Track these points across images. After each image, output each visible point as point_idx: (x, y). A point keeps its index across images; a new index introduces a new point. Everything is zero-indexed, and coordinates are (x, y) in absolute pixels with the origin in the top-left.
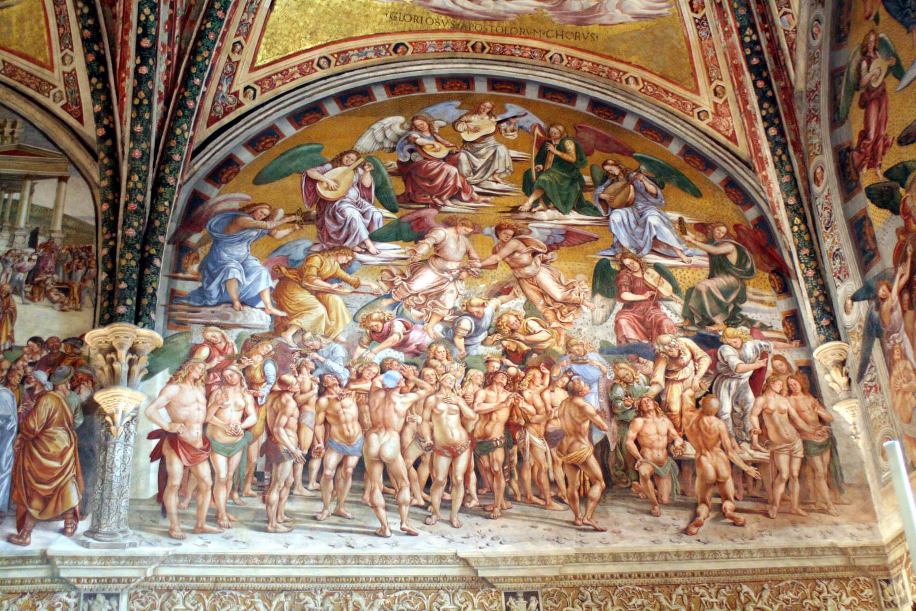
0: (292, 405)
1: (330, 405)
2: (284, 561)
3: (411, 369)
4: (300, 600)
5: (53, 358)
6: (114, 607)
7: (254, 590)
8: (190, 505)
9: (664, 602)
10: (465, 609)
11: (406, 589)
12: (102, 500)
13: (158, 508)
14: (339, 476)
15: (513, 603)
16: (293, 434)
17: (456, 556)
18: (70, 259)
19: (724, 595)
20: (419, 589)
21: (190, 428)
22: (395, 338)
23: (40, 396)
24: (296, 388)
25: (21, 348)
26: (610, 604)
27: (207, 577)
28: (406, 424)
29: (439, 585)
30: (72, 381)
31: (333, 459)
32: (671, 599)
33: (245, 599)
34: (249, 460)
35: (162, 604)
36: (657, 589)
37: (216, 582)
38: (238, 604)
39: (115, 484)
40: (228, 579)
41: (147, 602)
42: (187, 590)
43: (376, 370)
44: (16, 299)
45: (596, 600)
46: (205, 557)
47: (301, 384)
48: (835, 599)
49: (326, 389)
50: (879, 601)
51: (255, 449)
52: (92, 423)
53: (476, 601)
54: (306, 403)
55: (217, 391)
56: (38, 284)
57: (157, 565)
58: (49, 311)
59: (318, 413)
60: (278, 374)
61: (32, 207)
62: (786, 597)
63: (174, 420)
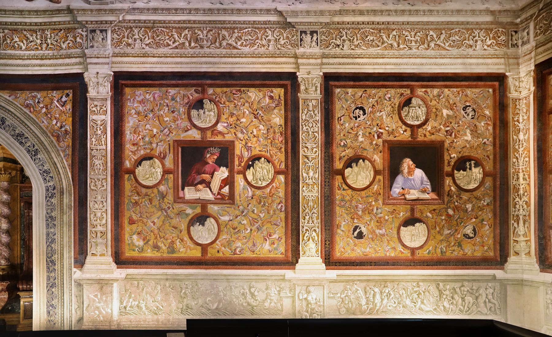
2: (188, 12)
4: (195, 33)
6: (105, 36)
7: (173, 28)
9: (385, 39)
10: (279, 39)
11: (249, 28)
15: (304, 37)
17: (276, 9)
19: (419, 36)
20: (255, 28)
26: (355, 39)
27: (150, 21)
29: (266, 26)
32: (389, 37)
33: (168, 32)
35: (128, 35)
36: (382, 31)
37: (154, 23)
38: (165, 35)
40: (160, 22)
41: (120, 34)
42: (139, 28)
45: (348, 37)
46: (148, 9)
48: (482, 41)
50: (508, 43)
53: (285, 35)
57: (124, 14)
62: (454, 39)
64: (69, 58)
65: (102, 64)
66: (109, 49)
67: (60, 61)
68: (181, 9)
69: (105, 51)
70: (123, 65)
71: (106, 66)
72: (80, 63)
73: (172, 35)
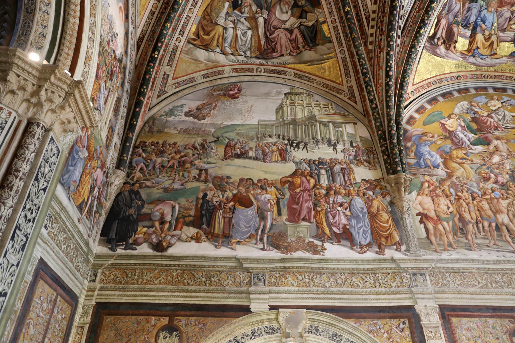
0: (464, 204)
1: (478, 204)
3: (503, 191)
5: (372, 187)
8: (440, 240)
12: (407, 238)
13: (429, 241)
14: (491, 230)
16: (468, 214)
18: (367, 152)
21: (430, 212)
22: (492, 180)
23: (372, 200)
24: (463, 197)
25: (360, 183)
28: (508, 211)
30: (382, 195)
31: (486, 224)
34: (456, 224)
39: (410, 233)
43: (490, 191)
44: (352, 166)
46: (452, 260)
47: (465, 196)
49: (474, 198)
51: (456, 219)
52: (394, 210)
54: (469, 203)
55: (436, 199)
56: (358, 160)
58: (365, 170)
59: (474, 207)
60: (455, 193)
61: (348, 133)
63: (424, 209)
64: (400, 294)
65: (428, 299)
66: (431, 288)
67: (393, 296)
68: (476, 260)
69: (428, 289)
70: (444, 300)
71: (431, 301)
72: (410, 298)
73: (476, 278)
